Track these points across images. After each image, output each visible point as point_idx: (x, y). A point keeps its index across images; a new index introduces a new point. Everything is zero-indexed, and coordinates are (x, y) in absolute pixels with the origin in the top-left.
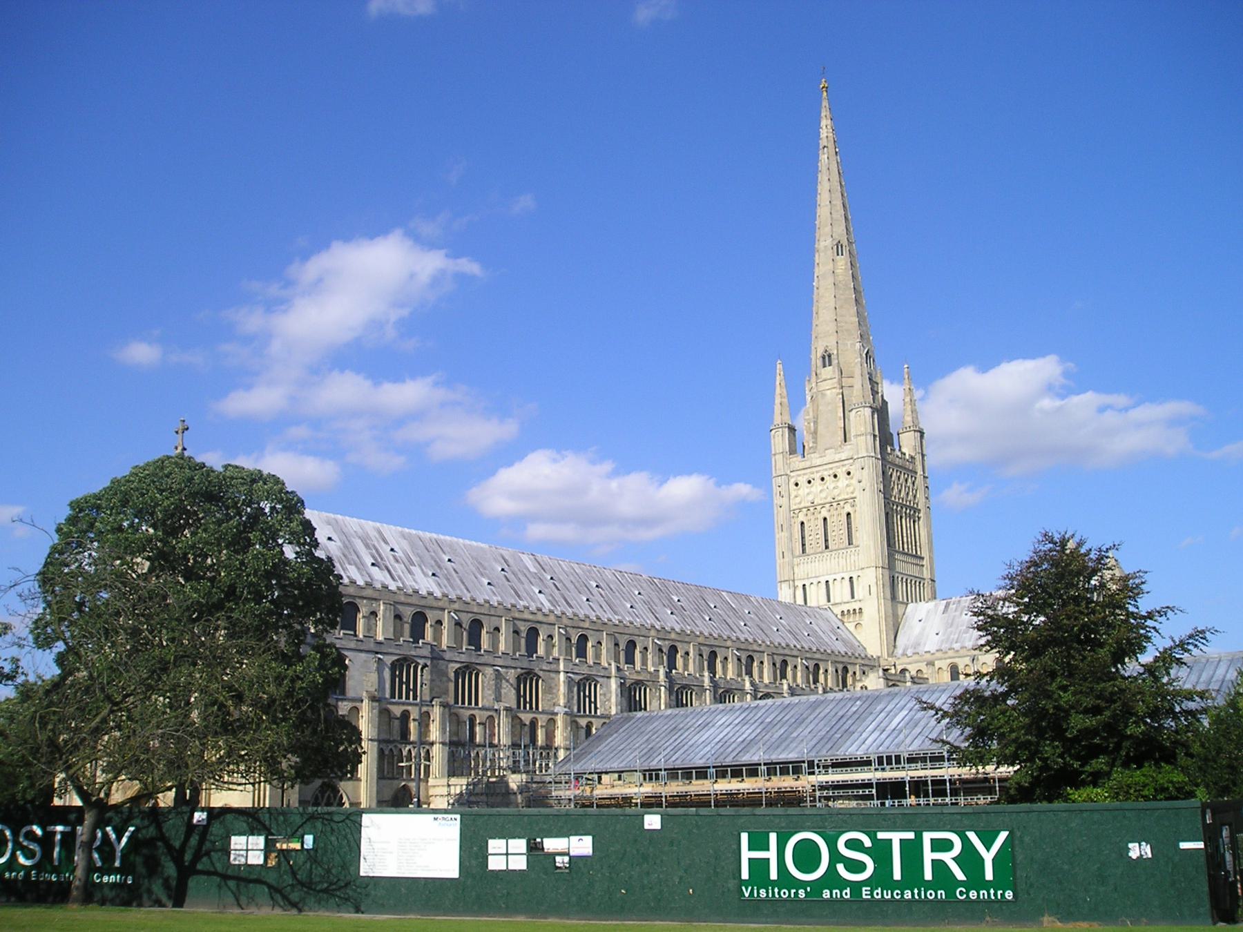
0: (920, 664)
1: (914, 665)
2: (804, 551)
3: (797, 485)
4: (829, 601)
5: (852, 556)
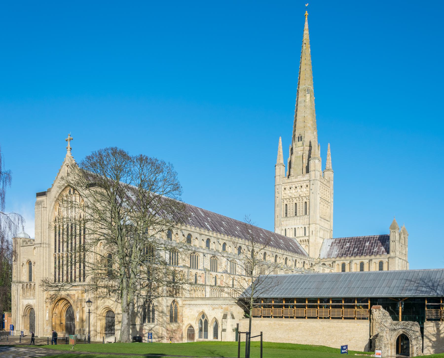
0: (330, 262)
1: (327, 262)
2: (286, 216)
3: (285, 189)
4: (295, 235)
5: (305, 219)
